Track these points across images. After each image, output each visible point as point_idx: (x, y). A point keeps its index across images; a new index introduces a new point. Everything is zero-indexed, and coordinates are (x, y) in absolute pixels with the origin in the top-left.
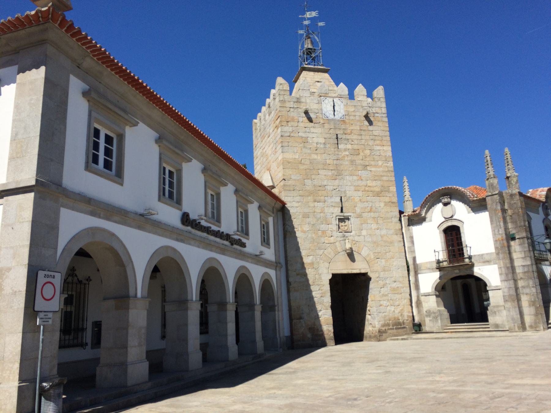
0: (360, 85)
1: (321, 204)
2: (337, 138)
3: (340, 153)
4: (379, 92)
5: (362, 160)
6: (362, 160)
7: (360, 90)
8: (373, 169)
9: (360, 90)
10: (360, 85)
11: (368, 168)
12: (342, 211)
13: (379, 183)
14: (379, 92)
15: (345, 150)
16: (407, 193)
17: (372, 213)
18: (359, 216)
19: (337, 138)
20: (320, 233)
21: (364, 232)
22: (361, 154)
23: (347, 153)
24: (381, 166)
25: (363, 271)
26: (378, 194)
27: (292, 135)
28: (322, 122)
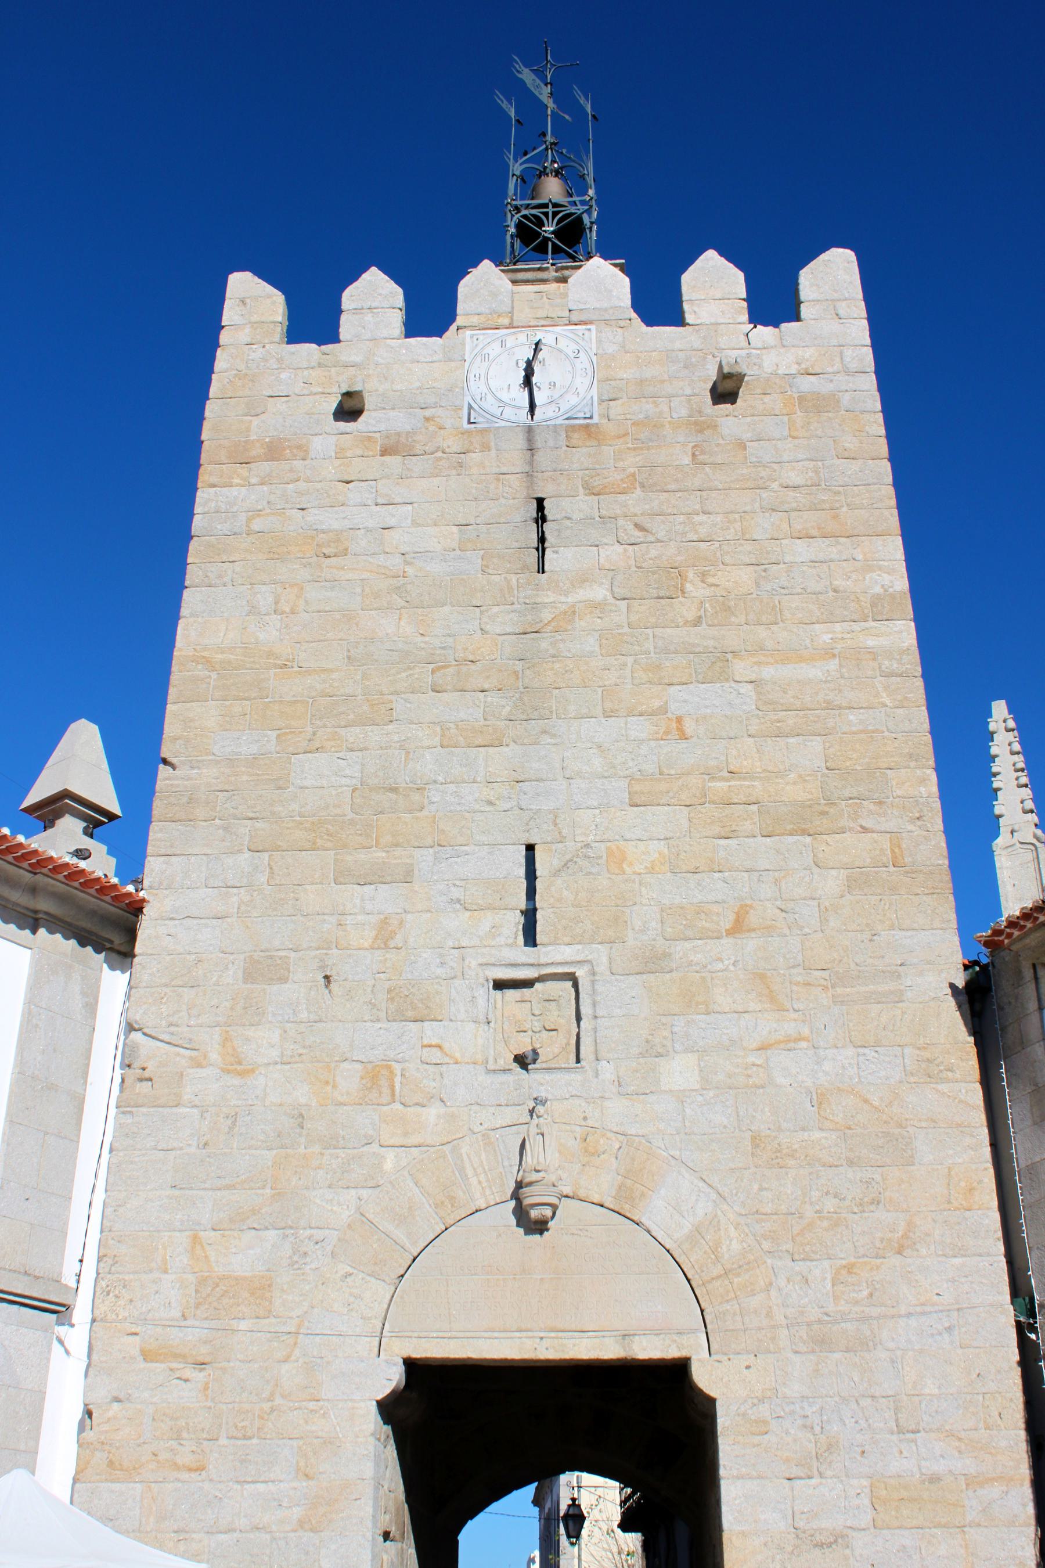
0: (711, 257)
1: (383, 899)
2: (541, 518)
3: (549, 597)
4: (832, 280)
5: (697, 622)
6: (697, 622)
7: (713, 283)
8: (768, 672)
9: (713, 283)
10: (711, 257)
11: (741, 668)
12: (530, 936)
13: (810, 753)
14: (832, 280)
15: (583, 579)
16: (1012, 797)
17: (751, 944)
18: (652, 963)
19: (541, 518)
20: (349, 1080)
21: (679, 1072)
22: (695, 589)
23: (599, 592)
24: (829, 653)
25: (648, 1349)
26: (804, 822)
27: (256, 526)
28: (454, 444)
